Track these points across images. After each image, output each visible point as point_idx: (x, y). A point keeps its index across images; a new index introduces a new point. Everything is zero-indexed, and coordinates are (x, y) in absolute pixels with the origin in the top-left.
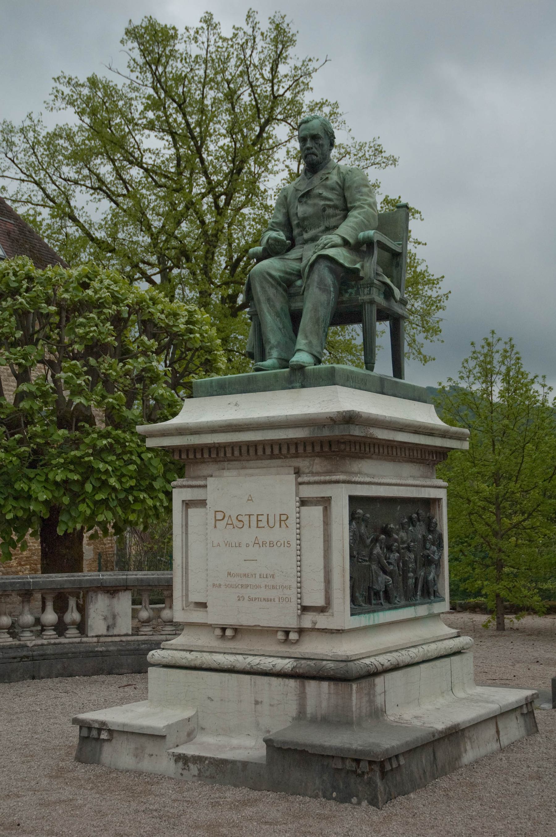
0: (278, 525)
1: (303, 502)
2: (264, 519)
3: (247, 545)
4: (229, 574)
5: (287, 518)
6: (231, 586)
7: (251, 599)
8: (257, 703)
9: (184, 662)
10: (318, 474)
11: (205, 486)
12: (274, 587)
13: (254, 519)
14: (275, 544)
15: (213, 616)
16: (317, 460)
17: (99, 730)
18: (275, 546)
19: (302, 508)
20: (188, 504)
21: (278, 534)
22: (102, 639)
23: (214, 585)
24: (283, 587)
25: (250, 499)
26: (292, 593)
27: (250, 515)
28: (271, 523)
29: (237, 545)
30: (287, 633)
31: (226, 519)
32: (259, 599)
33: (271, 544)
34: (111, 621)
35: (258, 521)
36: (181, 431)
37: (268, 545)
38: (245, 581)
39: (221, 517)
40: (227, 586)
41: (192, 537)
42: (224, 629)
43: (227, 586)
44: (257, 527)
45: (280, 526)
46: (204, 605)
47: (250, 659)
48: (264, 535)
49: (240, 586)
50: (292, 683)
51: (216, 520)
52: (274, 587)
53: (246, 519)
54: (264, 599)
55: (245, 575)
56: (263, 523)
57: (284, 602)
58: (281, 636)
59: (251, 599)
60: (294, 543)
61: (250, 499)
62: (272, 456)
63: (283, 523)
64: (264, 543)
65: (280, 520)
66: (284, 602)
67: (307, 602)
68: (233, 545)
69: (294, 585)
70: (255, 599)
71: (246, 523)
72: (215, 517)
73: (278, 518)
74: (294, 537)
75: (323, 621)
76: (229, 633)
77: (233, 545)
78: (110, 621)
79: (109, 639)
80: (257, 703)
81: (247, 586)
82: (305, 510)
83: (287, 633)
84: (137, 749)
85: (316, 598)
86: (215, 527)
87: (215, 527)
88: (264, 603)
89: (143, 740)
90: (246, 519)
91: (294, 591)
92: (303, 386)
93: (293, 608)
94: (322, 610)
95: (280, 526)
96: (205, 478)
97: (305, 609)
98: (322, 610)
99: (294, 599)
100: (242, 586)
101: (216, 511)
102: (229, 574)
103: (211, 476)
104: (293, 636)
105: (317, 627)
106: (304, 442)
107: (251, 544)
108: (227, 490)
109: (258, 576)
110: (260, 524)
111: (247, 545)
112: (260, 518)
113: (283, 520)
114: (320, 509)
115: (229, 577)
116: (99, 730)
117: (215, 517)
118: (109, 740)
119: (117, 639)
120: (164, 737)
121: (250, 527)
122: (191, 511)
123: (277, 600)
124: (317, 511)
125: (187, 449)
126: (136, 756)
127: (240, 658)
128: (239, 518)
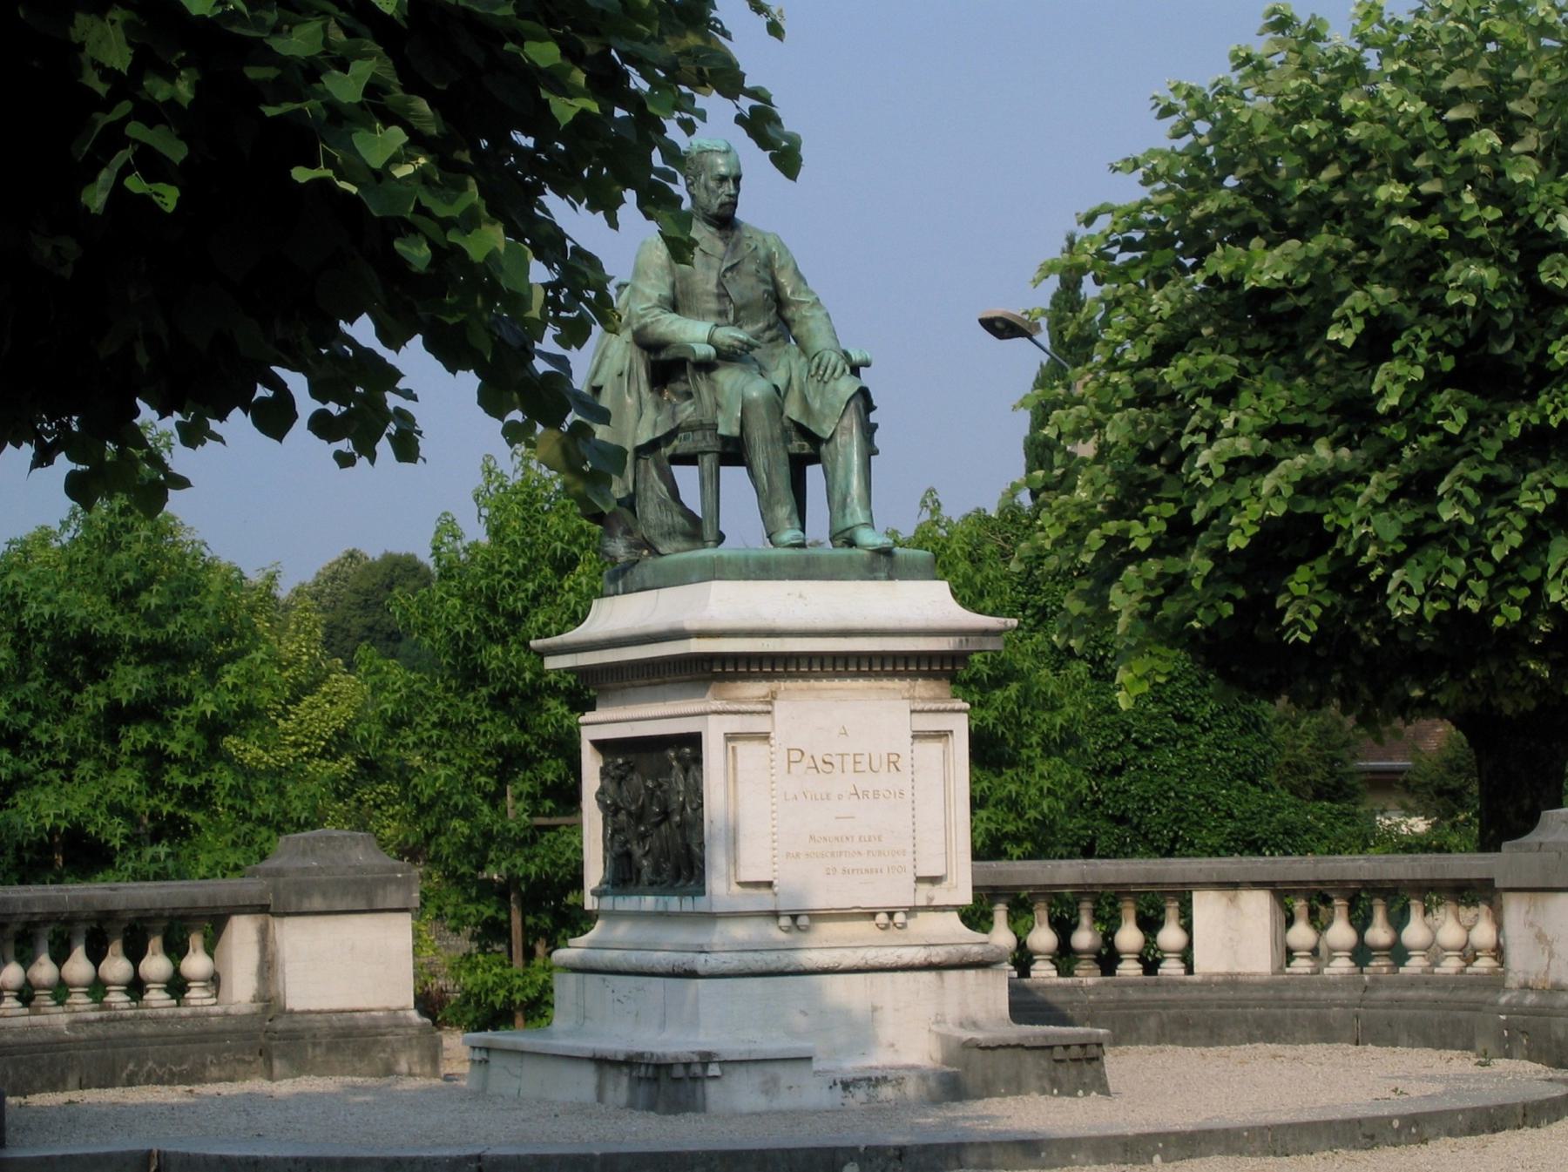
3: (840, 797)
9: (756, 967)
10: (923, 699)
13: (849, 760)
16: (920, 681)
17: (705, 1065)
20: (731, 737)
23: (788, 855)
28: (875, 765)
32: (860, 871)
33: (876, 794)
39: (796, 755)
47: (861, 953)
53: (836, 761)
56: (864, 766)
58: (882, 918)
60: (908, 795)
64: (865, 793)
69: (911, 849)
71: (837, 764)
75: (941, 896)
84: (765, 1083)
89: (778, 1069)
92: (890, 578)
105: (935, 903)
110: (859, 767)
122: (742, 747)
124: (934, 747)
126: (766, 1092)
127: (848, 952)
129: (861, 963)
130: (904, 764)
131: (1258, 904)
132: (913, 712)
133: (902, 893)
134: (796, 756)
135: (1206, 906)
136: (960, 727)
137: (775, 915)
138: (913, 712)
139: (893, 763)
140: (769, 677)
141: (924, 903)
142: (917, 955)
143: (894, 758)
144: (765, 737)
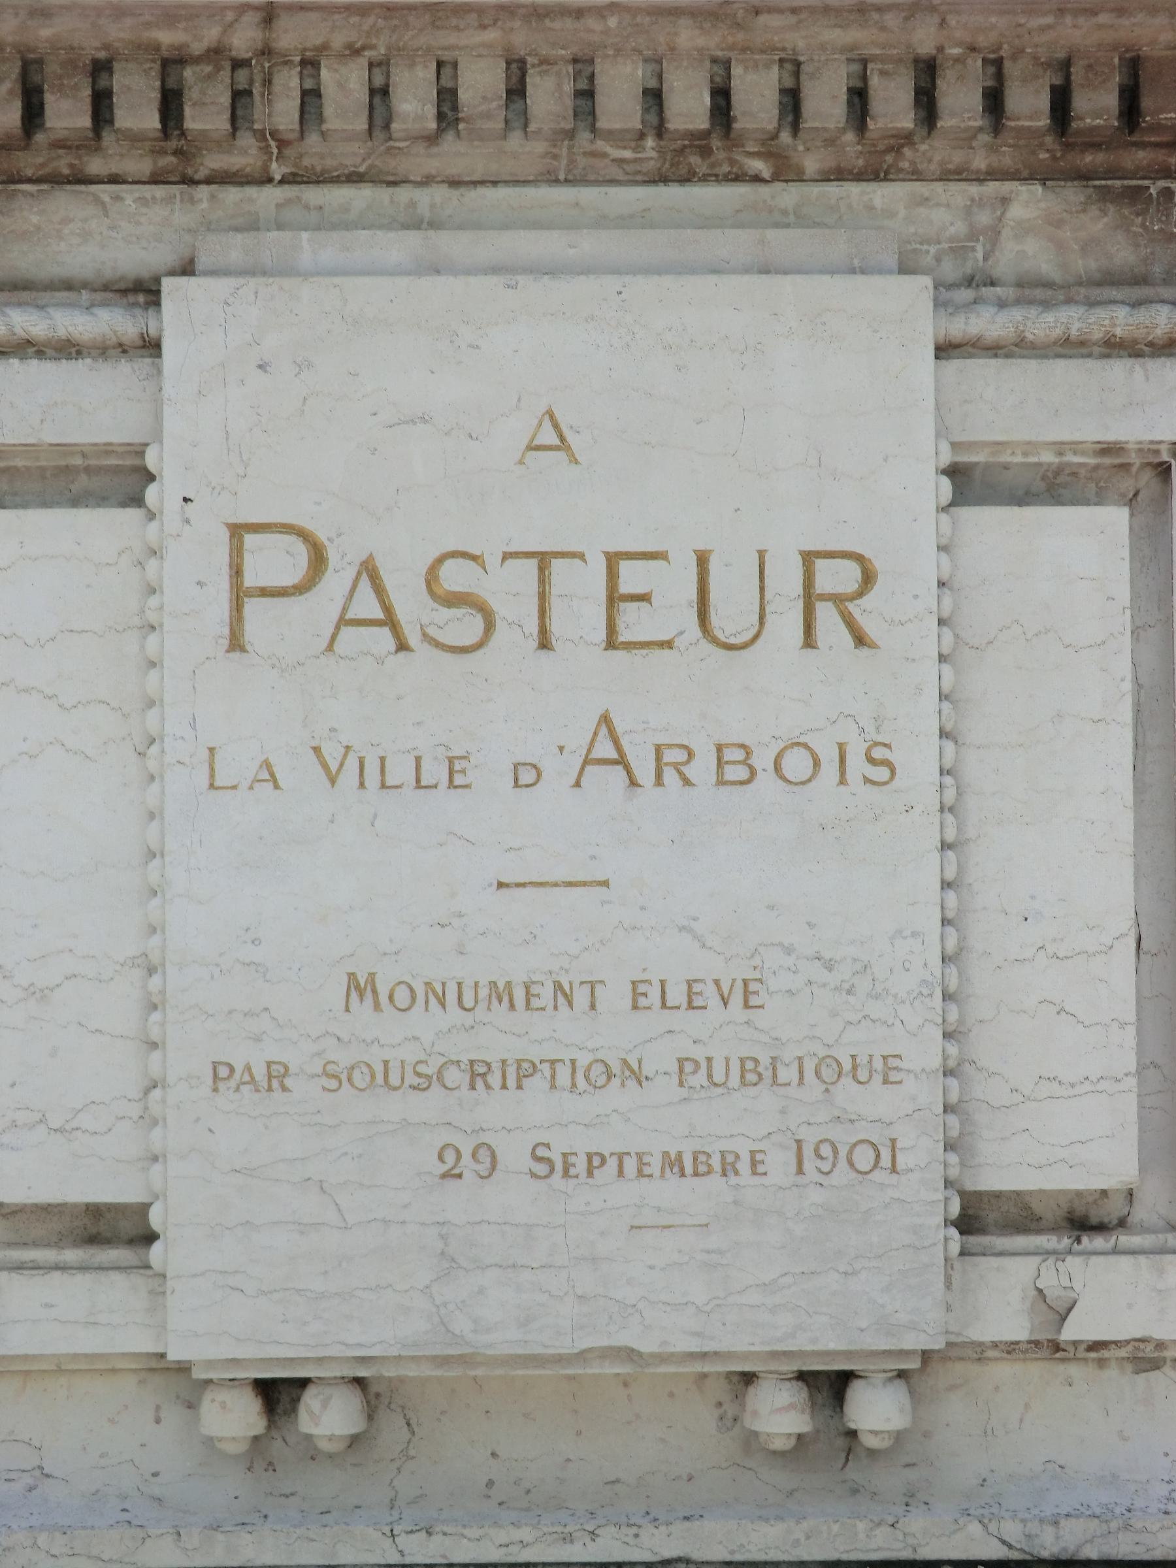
0: (786, 623)
1: (968, 483)
2: (674, 585)
3: (527, 776)
4: (360, 988)
5: (868, 578)
6: (383, 1080)
10: (1035, 290)
11: (152, 347)
12: (752, 1073)
14: (763, 760)
16: (1028, 202)
18: (766, 780)
19: (970, 515)
21: (786, 691)
24: (833, 1070)
25: (554, 440)
26: (906, 1112)
27: (543, 560)
28: (731, 618)
29: (435, 772)
31: (336, 583)
33: (734, 765)
35: (614, 598)
37: (702, 769)
38: (500, 1038)
39: (277, 568)
40: (335, 1077)
42: (277, 1395)
43: (335, 1077)
44: (612, 643)
45: (809, 640)
46: (115, 1232)
48: (665, 702)
49: (454, 1076)
51: (239, 595)
52: (752, 1073)
53: (509, 591)
54: (673, 1163)
55: (501, 994)
57: (842, 1175)
58: (780, 1414)
60: (919, 760)
63: (826, 614)
64: (671, 762)
65: (810, 598)
66: (842, 1175)
67: (1005, 1170)
68: (402, 772)
69: (925, 1052)
70: (595, 1162)
72: (237, 572)
73: (786, 580)
74: (926, 714)
76: (327, 1417)
77: (402, 772)
81: (525, 1071)
82: (988, 524)
86: (236, 643)
87: (236, 643)
88: (668, 1192)
90: (509, 591)
91: (928, 1094)
93: (919, 1206)
95: (809, 640)
97: (975, 1218)
99: (921, 1151)
100: (477, 1074)
101: (237, 531)
102: (360, 988)
104: (875, 1410)
105: (1069, 1333)
107: (559, 771)
109: (615, 996)
110: (636, 623)
111: (527, 776)
112: (631, 578)
113: (832, 596)
114: (1114, 519)
115: (363, 1010)
117: (237, 572)
121: (544, 643)
123: (778, 1162)
128: (454, 577)
130: (901, 607)
132: (944, 350)
133: (876, 1286)
134: (276, 561)
138: (944, 350)
139: (832, 596)
140: (177, 161)
141: (1018, 1329)
143: (836, 577)
144: (122, 479)
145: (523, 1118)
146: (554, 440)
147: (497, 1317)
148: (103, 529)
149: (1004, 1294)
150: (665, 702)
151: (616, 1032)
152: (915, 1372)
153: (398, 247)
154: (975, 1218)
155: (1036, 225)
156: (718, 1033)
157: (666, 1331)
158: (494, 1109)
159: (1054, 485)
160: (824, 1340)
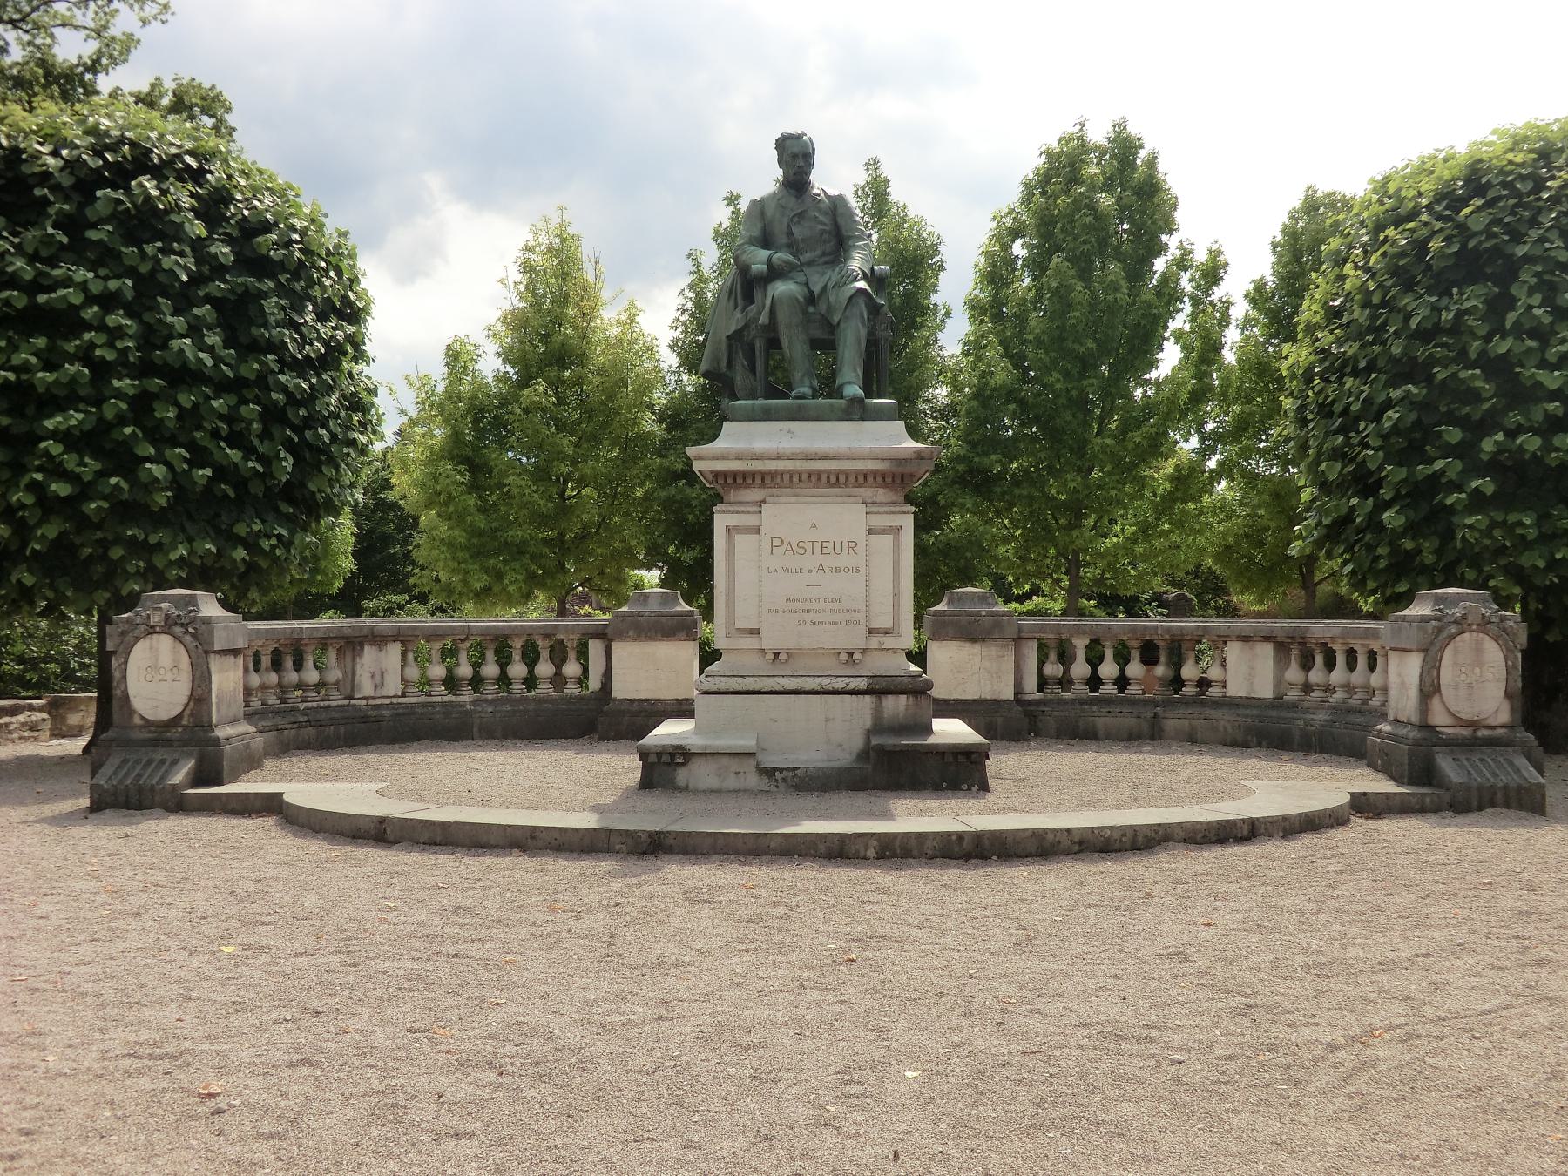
1: (870, 531)
3: (810, 571)
7: (813, 623)
8: (827, 720)
9: (738, 688)
12: (840, 611)
13: (818, 547)
15: (769, 642)
16: (881, 490)
21: (845, 560)
22: (372, 702)
26: (861, 616)
30: (851, 654)
34: (379, 679)
36: (723, 457)
38: (807, 606)
41: (739, 564)
42: (776, 654)
46: (755, 632)
47: (818, 680)
48: (829, 561)
50: (868, 698)
52: (840, 611)
53: (808, 546)
58: (844, 657)
59: (813, 623)
60: (863, 569)
61: (814, 526)
62: (837, 484)
75: (889, 642)
76: (783, 657)
78: (378, 678)
79: (378, 702)
80: (827, 720)
83: (851, 654)
85: (886, 622)
90: (808, 546)
93: (863, 629)
94: (886, 632)
96: (760, 503)
97: (870, 631)
98: (886, 632)
99: (863, 622)
103: (764, 501)
104: (857, 657)
106: (875, 473)
108: (785, 517)
111: (810, 571)
113: (851, 547)
114: (890, 537)
116: (672, 755)
118: (683, 764)
119: (387, 701)
120: (752, 754)
122: (738, 538)
125: (735, 474)
129: (818, 688)
130: (861, 548)
131: (1266, 651)
133: (857, 640)
135: (1233, 651)
136: (908, 523)
137: (763, 651)
140: (763, 485)
142: (862, 684)
144: (757, 530)
145: (809, 617)
146: (814, 526)
147: (806, 644)
148: (755, 537)
149: (874, 642)
150: (829, 561)
151: (822, 605)
152: (863, 652)
153: (793, 499)
154: (870, 631)
155: (882, 494)
156: (836, 606)
157: (828, 646)
158: (805, 615)
159: (883, 531)
160: (850, 647)
